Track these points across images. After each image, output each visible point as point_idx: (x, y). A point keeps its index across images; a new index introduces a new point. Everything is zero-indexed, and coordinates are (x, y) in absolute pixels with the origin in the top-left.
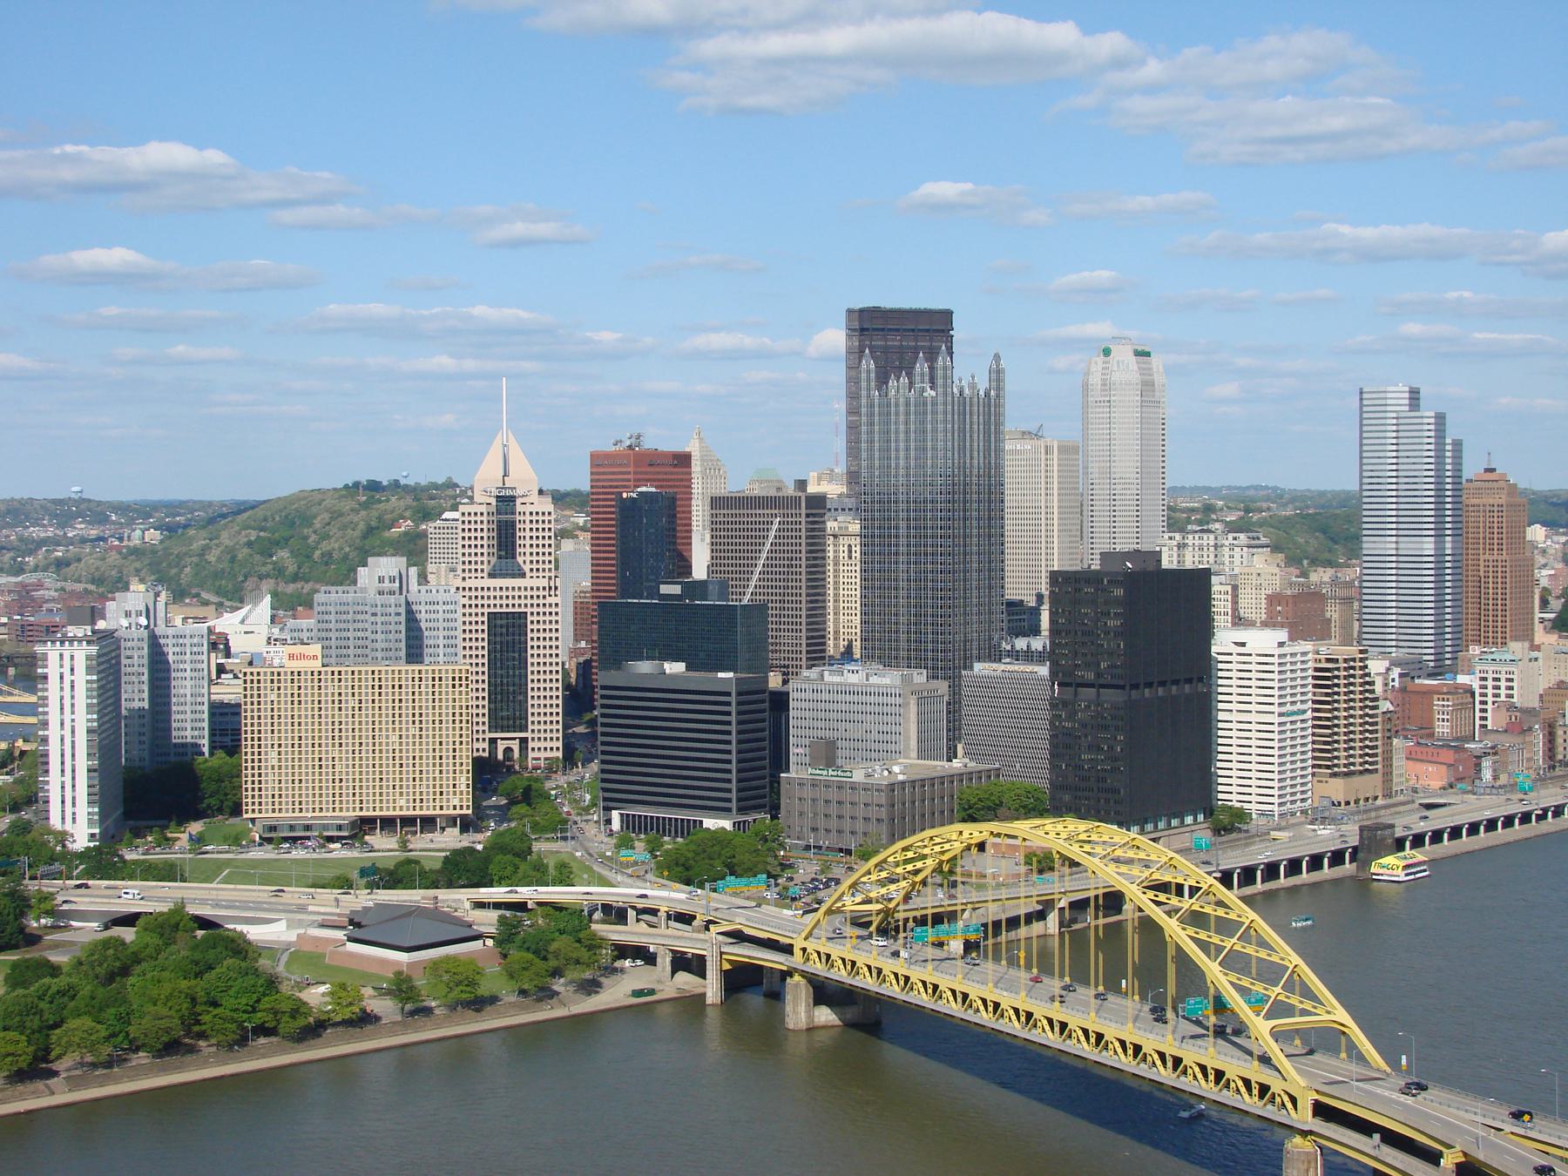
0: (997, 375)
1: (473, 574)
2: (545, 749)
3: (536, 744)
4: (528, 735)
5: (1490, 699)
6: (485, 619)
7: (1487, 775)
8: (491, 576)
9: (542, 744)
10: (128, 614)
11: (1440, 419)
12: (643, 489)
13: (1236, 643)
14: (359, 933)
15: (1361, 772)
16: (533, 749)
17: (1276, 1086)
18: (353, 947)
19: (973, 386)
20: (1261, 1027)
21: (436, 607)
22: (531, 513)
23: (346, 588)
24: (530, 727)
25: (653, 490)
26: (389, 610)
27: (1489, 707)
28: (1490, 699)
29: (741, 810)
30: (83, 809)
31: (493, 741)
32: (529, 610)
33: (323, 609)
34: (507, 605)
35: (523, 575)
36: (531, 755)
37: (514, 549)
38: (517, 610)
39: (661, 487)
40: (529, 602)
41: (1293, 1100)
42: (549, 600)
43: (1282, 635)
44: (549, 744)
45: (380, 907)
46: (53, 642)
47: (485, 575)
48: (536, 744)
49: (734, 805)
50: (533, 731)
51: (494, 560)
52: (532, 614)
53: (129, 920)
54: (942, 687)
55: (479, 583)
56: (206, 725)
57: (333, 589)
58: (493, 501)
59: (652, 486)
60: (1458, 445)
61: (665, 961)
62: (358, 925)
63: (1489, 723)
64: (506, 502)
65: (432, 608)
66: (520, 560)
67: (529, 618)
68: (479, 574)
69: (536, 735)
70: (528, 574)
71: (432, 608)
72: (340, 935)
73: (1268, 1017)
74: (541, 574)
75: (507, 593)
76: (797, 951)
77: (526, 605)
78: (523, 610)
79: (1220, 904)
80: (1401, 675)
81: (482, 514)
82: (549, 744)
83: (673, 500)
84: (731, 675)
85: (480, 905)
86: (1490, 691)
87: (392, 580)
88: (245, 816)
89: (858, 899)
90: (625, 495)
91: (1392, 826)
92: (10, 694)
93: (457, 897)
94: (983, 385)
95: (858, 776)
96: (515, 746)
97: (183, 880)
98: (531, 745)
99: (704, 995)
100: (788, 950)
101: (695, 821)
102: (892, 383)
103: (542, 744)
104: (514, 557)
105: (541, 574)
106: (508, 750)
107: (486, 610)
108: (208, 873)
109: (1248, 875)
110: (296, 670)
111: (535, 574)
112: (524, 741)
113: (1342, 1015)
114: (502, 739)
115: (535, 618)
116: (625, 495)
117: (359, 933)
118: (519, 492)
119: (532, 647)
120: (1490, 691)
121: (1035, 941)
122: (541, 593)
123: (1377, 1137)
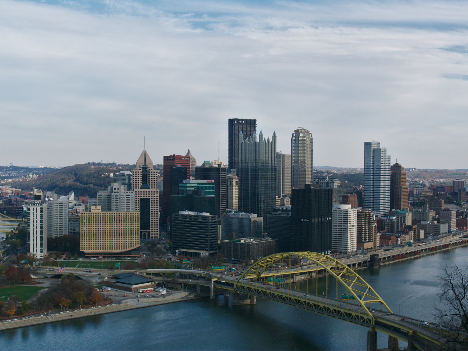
0: (274, 137)
1: (136, 188)
2: (154, 234)
3: (152, 233)
4: (150, 230)
5: (399, 223)
6: (139, 200)
7: (399, 243)
8: (141, 188)
9: (154, 233)
10: (48, 197)
11: (385, 150)
12: (178, 166)
13: (338, 208)
14: (118, 280)
15: (369, 242)
16: (151, 234)
17: (366, 317)
18: (117, 284)
19: (268, 140)
20: (363, 302)
21: (129, 196)
22: (151, 172)
23: (105, 191)
24: (151, 228)
25: (181, 166)
26: (117, 197)
27: (399, 225)
28: (399, 223)
29: (211, 250)
30: (39, 248)
31: (141, 232)
32: (151, 197)
33: (99, 196)
34: (148, 196)
35: (149, 188)
36: (151, 236)
37: (147, 182)
38: (147, 197)
39: (183, 165)
40: (147, 195)
41: (370, 321)
42: (156, 195)
43: (349, 206)
44: (155, 233)
45: (124, 274)
46: (32, 204)
47: (139, 188)
48: (152, 233)
49: (209, 249)
50: (151, 229)
51: (141, 184)
52: (151, 198)
53: (58, 276)
54: (261, 219)
55: (137, 190)
56: (67, 226)
57: (102, 191)
58: (142, 169)
59: (180, 165)
60: (389, 157)
61: (198, 289)
62: (118, 279)
63: (399, 229)
64: (145, 169)
65: (128, 197)
66: (148, 184)
67: (151, 200)
68: (138, 188)
69: (152, 230)
70: (151, 188)
71: (128, 197)
72: (114, 281)
73: (363, 301)
74: (154, 188)
75: (145, 193)
76: (235, 287)
77: (150, 196)
78: (149, 197)
79: (350, 272)
80: (376, 216)
81: (139, 172)
82: (155, 233)
83: (186, 168)
84: (208, 214)
85: (148, 274)
86: (399, 221)
87: (118, 189)
88: (81, 250)
89: (251, 272)
90: (173, 168)
91: (378, 255)
92: (8, 218)
93: (142, 271)
94: (271, 140)
95: (242, 241)
96: (147, 233)
97: (69, 267)
98: (151, 233)
99: (210, 296)
100: (232, 285)
101: (198, 253)
102: (247, 138)
103: (154, 233)
104: (147, 184)
105: (154, 188)
106: (145, 235)
107: (139, 197)
108: (73, 265)
109: (354, 265)
110: (98, 213)
111: (152, 188)
112: (149, 232)
113: (381, 300)
114: (143, 231)
115: (152, 200)
116: (173, 168)
117: (118, 280)
118: (148, 166)
119: (151, 207)
120: (399, 221)
121: (291, 284)
122: (154, 193)
123: (392, 329)
